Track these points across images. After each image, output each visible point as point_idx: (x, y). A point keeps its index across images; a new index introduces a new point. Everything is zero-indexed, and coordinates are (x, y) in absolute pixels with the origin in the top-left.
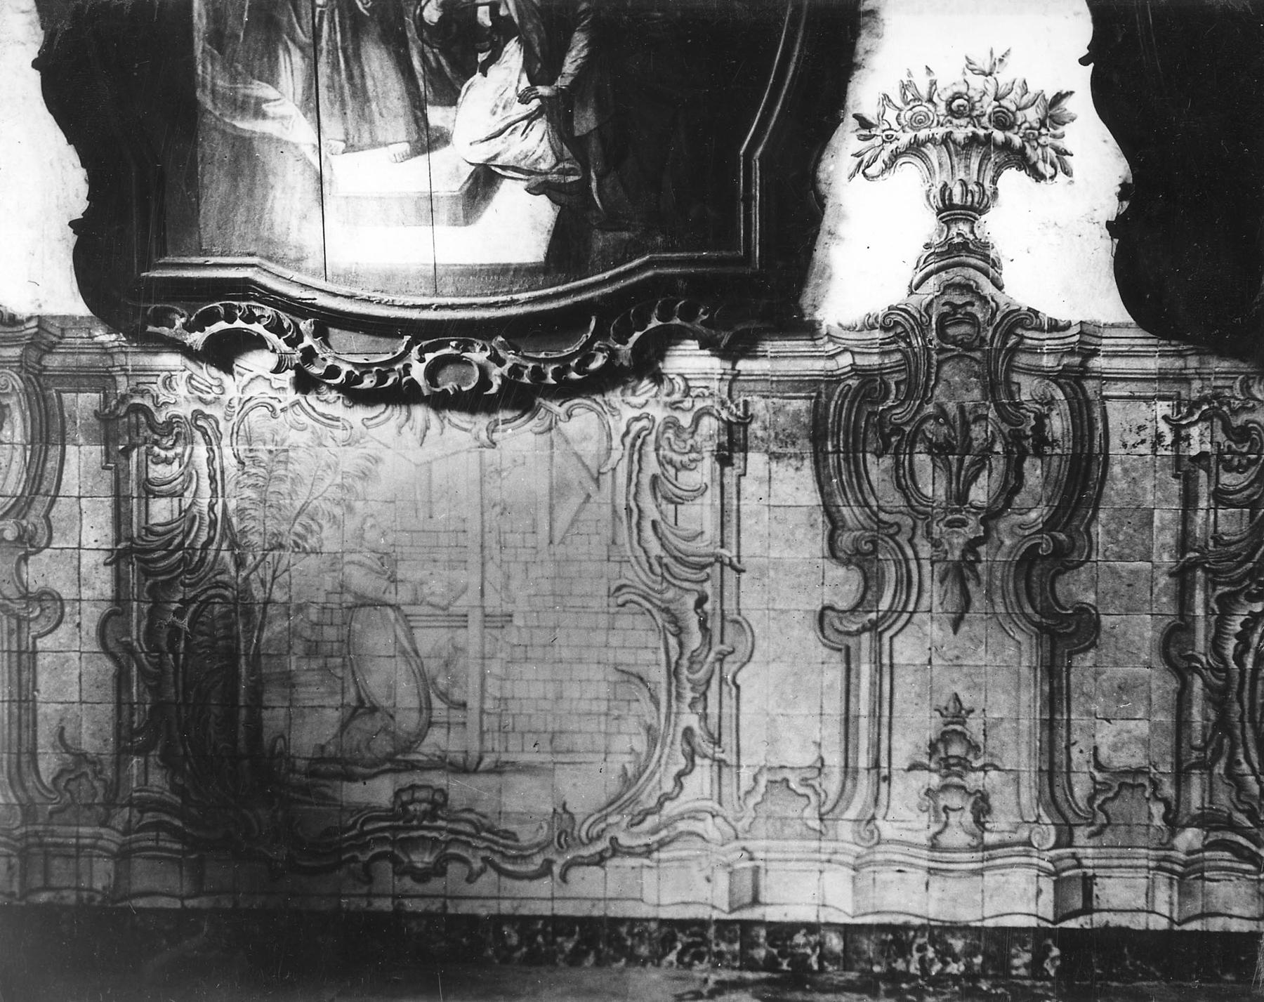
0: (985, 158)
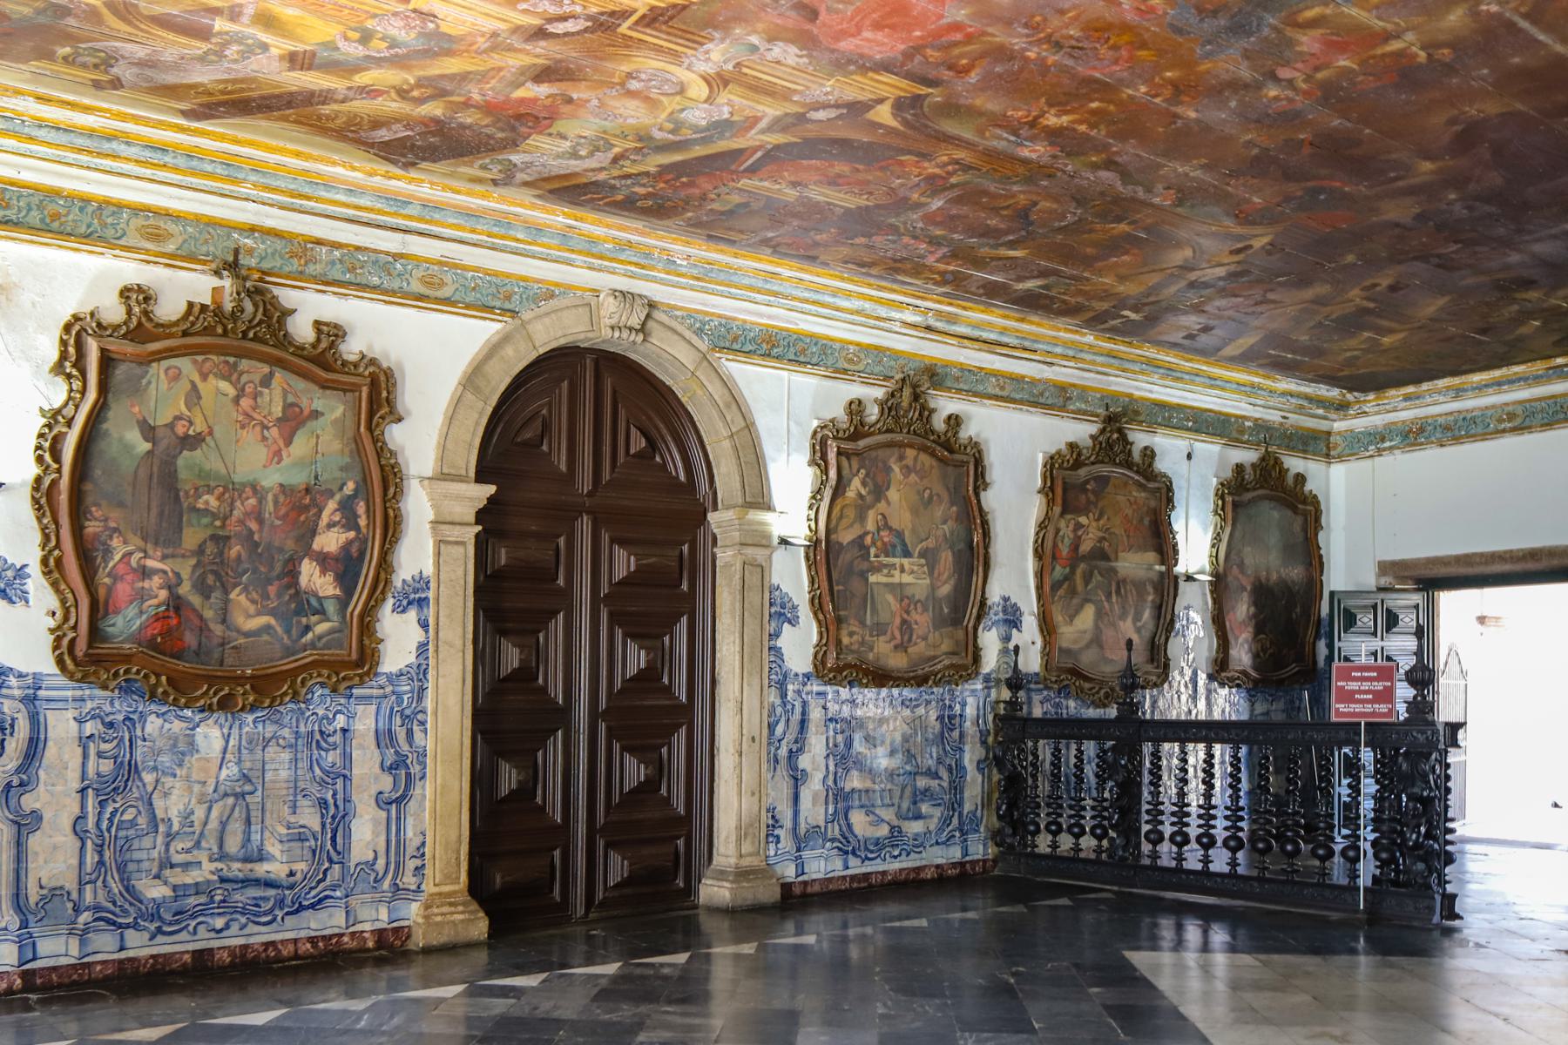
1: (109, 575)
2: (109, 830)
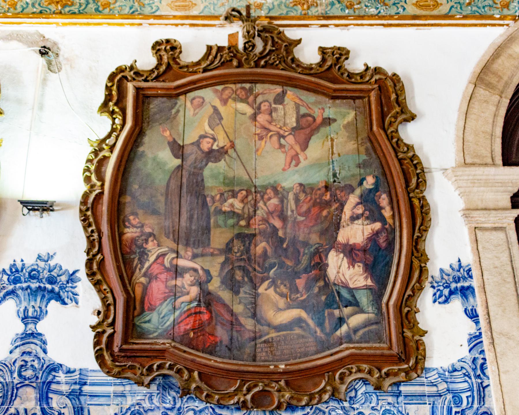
0: (43, 296)
1: (145, 275)
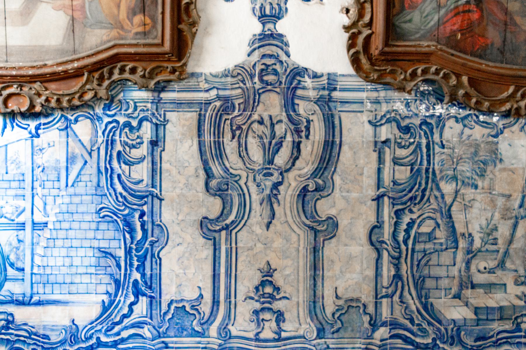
2: (405, 242)
